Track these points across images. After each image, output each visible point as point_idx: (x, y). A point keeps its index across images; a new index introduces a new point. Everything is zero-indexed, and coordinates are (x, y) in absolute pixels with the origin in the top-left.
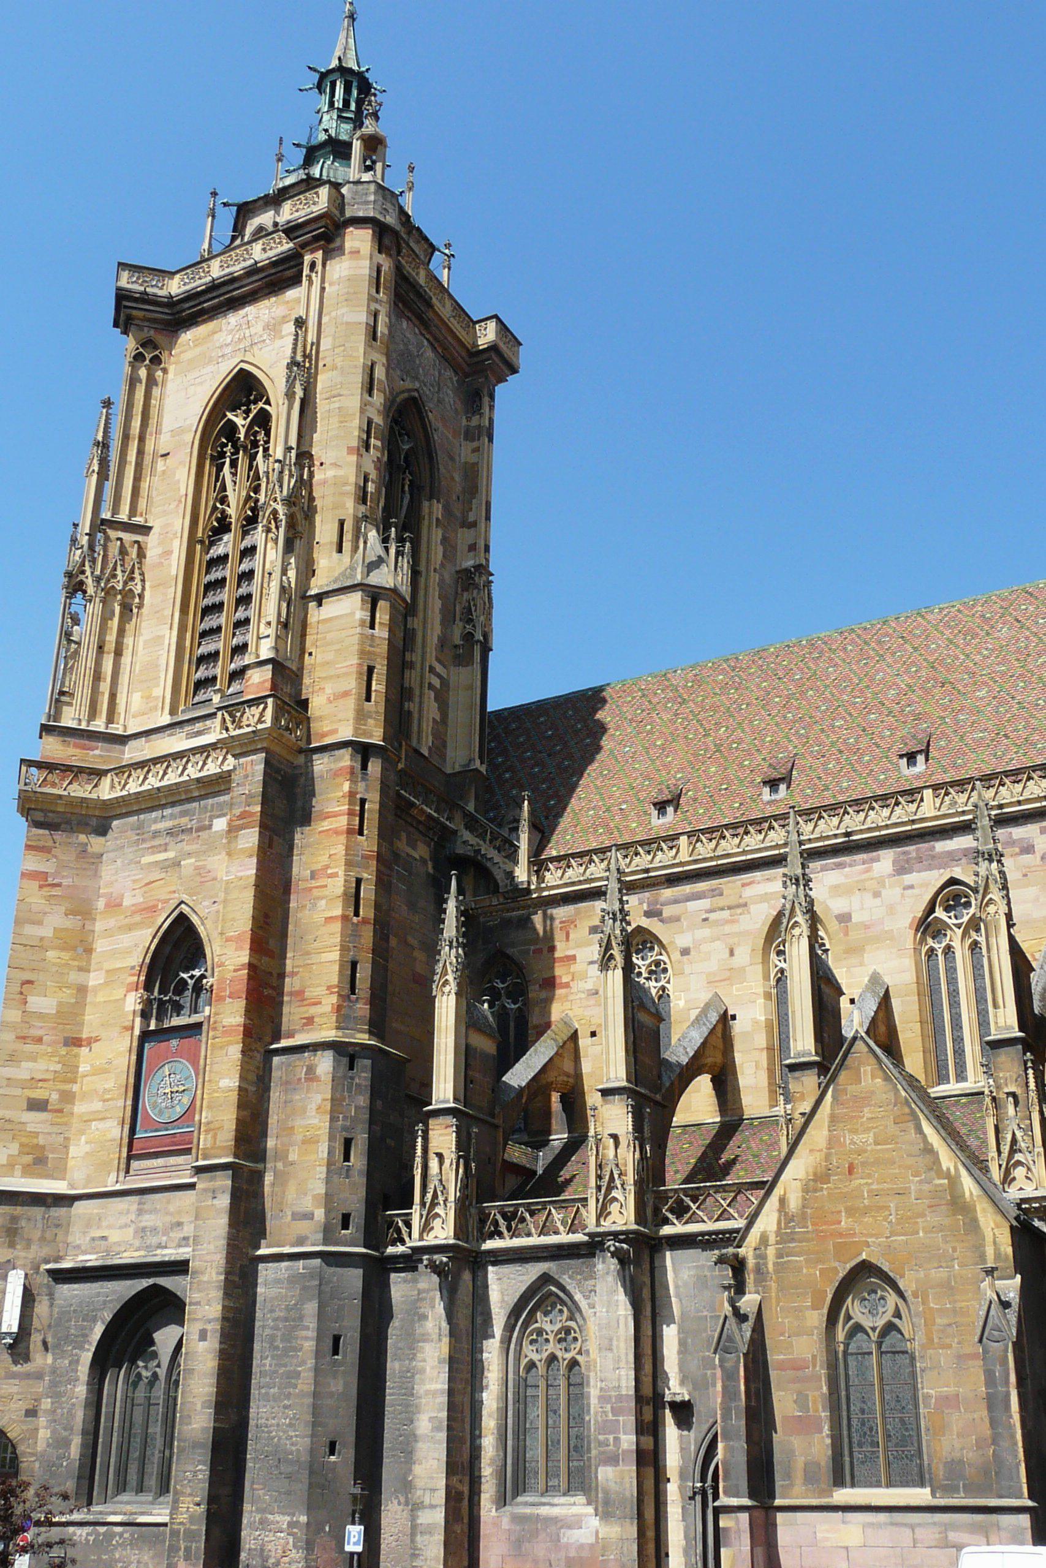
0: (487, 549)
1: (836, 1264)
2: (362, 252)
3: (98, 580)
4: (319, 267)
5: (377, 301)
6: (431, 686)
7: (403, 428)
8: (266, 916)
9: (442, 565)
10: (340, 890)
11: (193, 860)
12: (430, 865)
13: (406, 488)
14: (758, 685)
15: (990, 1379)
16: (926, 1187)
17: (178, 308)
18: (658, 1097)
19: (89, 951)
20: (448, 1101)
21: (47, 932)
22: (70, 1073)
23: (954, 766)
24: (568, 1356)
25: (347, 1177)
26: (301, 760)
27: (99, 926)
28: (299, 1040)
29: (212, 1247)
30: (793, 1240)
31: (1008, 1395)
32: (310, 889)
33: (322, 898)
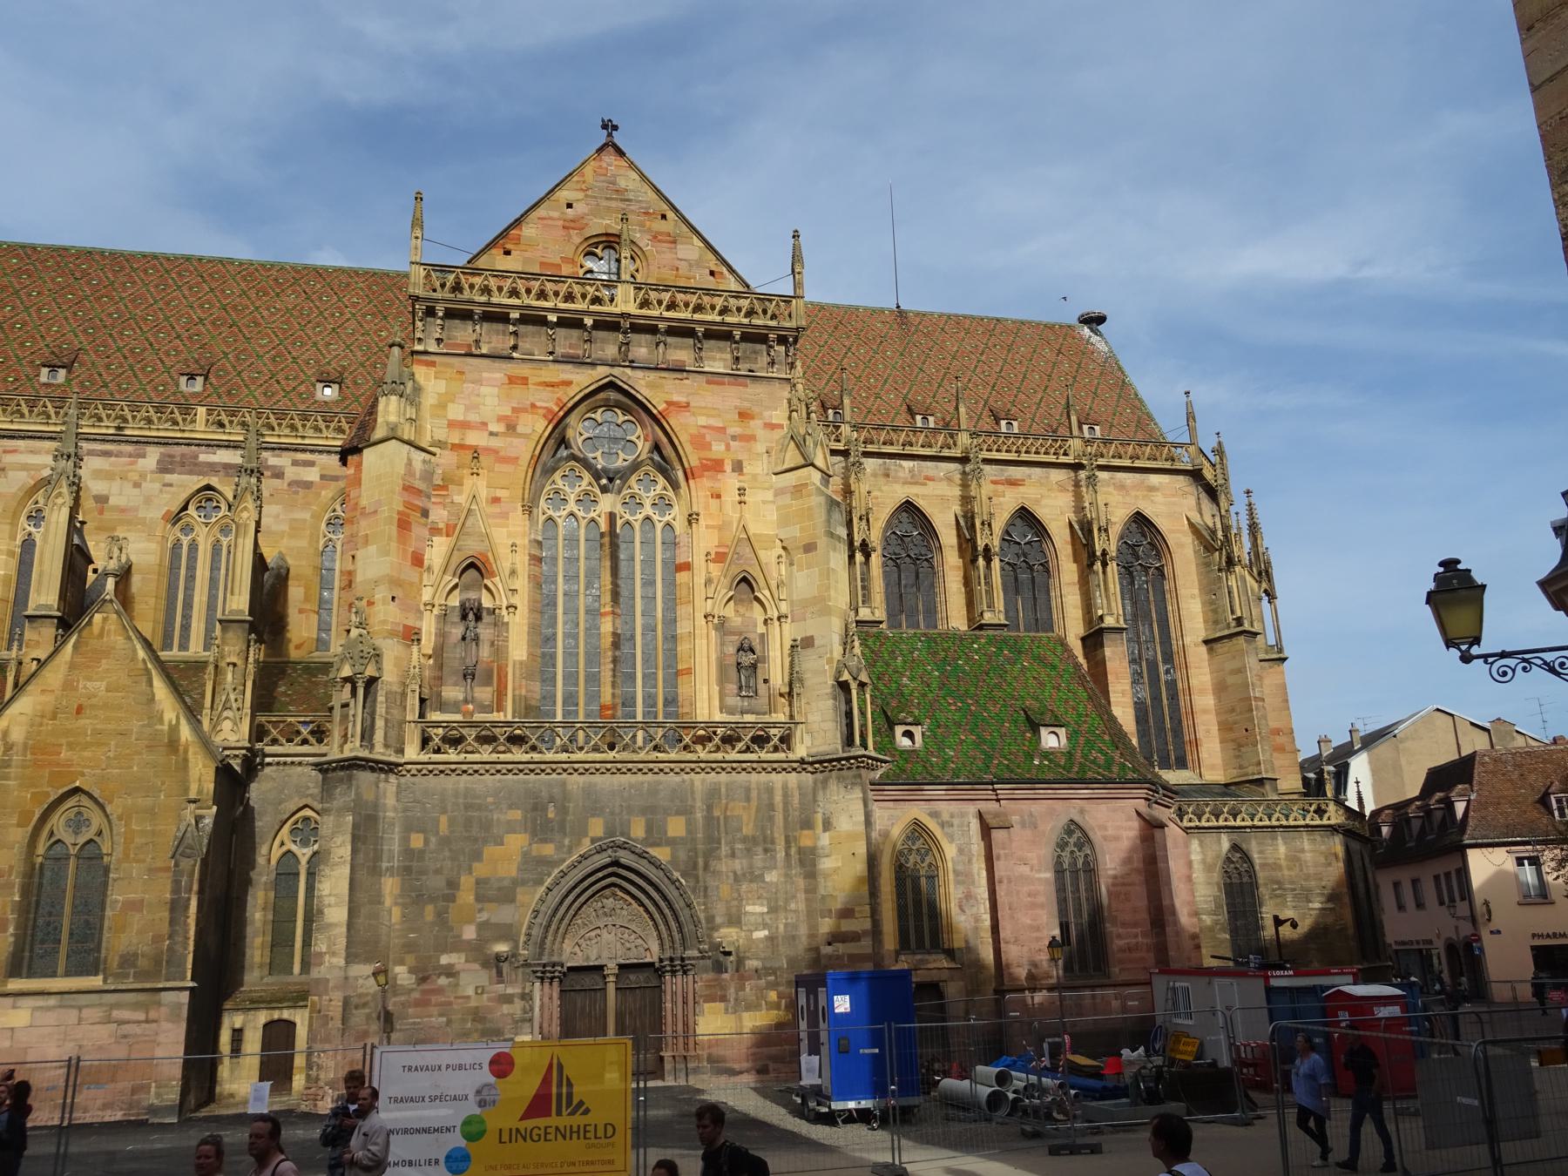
1: (49, 789)
14: (53, 280)
15: (176, 888)
30: (9, 766)
31: (189, 899)
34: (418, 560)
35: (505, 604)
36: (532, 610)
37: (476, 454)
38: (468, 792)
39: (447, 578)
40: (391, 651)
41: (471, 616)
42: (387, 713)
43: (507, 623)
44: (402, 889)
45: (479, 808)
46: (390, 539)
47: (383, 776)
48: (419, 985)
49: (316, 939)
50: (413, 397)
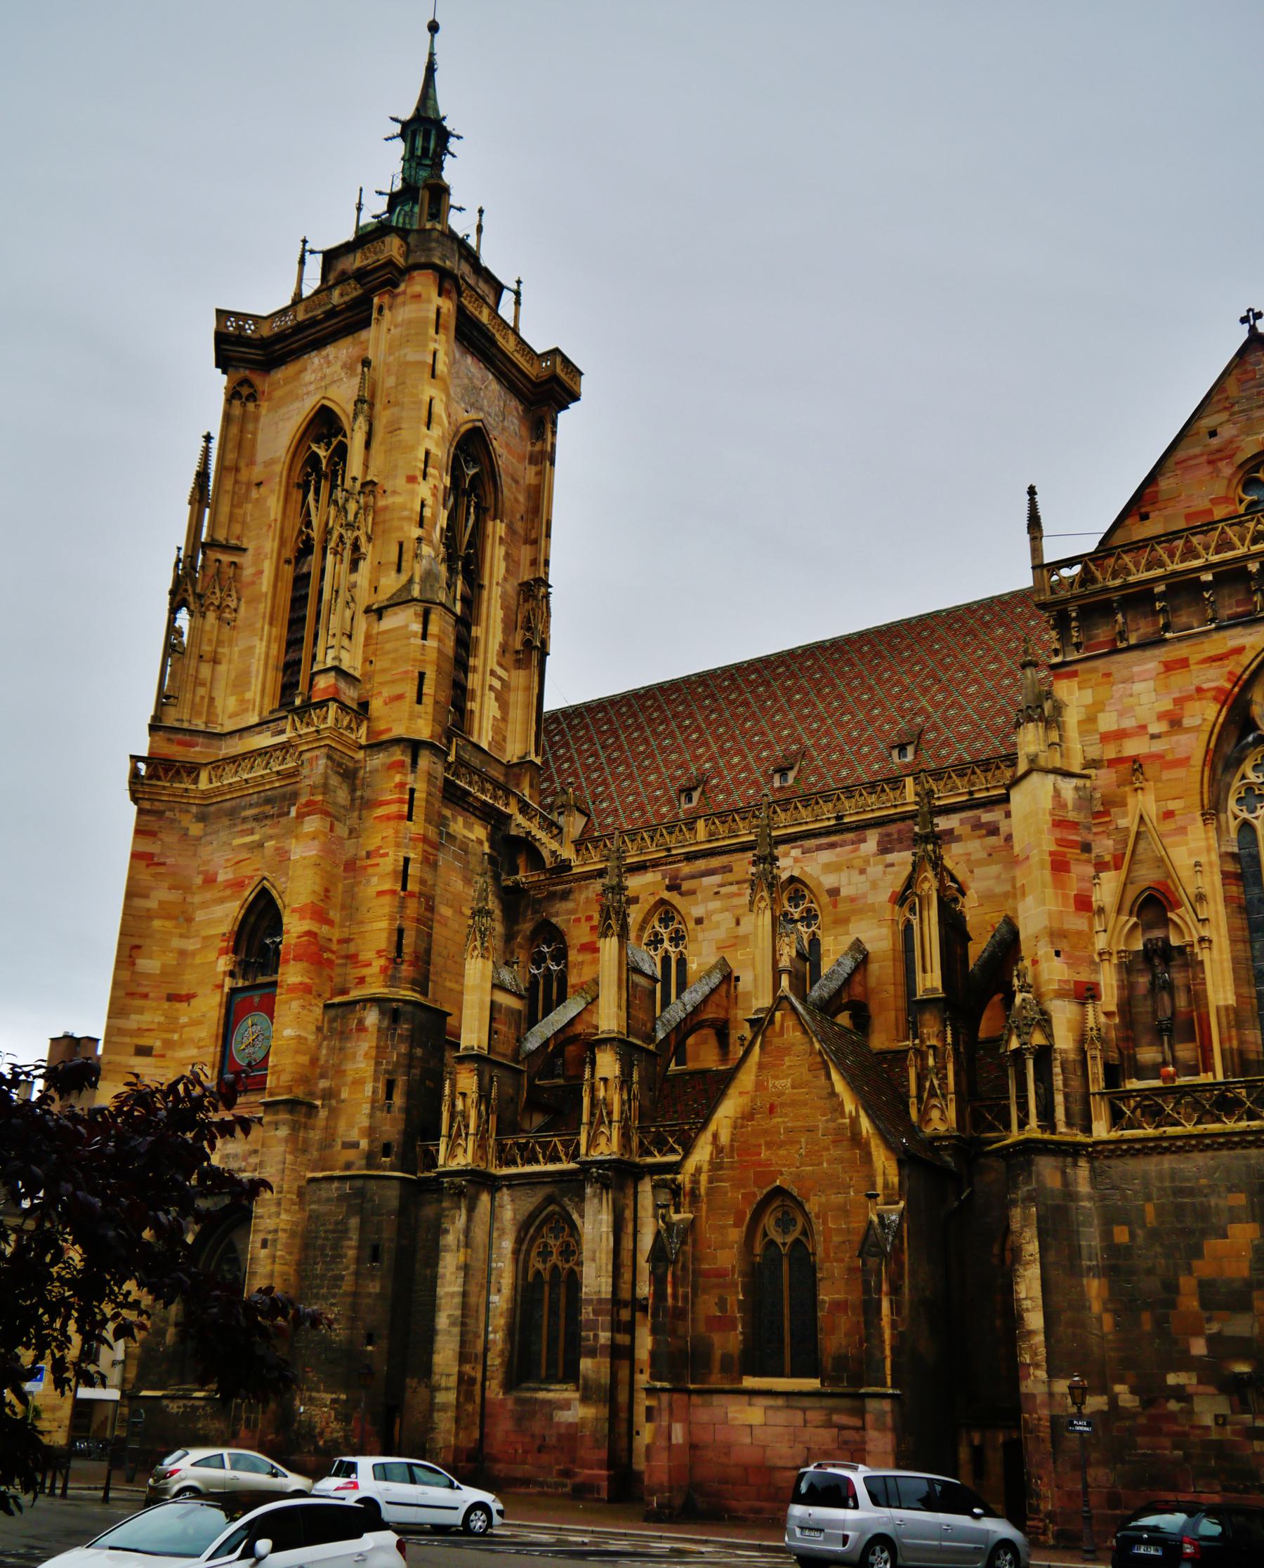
0: (547, 563)
3: (199, 596)
6: (491, 688)
7: (468, 455)
8: (327, 890)
9: (505, 579)
10: (390, 868)
11: (273, 843)
12: (486, 845)
13: (472, 510)
16: (832, 1125)
18: (652, 1047)
19: (189, 920)
20: (472, 1048)
21: (152, 904)
22: (171, 1025)
23: (936, 757)
24: (567, 1266)
25: (389, 1112)
26: (360, 755)
27: (197, 899)
28: (355, 994)
29: (273, 1171)
30: (721, 1168)
31: (880, 1301)
32: (365, 868)
33: (374, 875)
34: (1083, 903)
35: (1195, 940)
36: (1233, 941)
37: (1136, 765)
38: (1173, 1175)
39: (1124, 918)
40: (1063, 1015)
41: (1157, 962)
42: (1065, 1085)
43: (1202, 962)
44: (1111, 1289)
45: (1191, 1192)
46: (1044, 886)
47: (1069, 1160)
48: (1144, 1409)
49: (1021, 1349)
50: (1053, 721)
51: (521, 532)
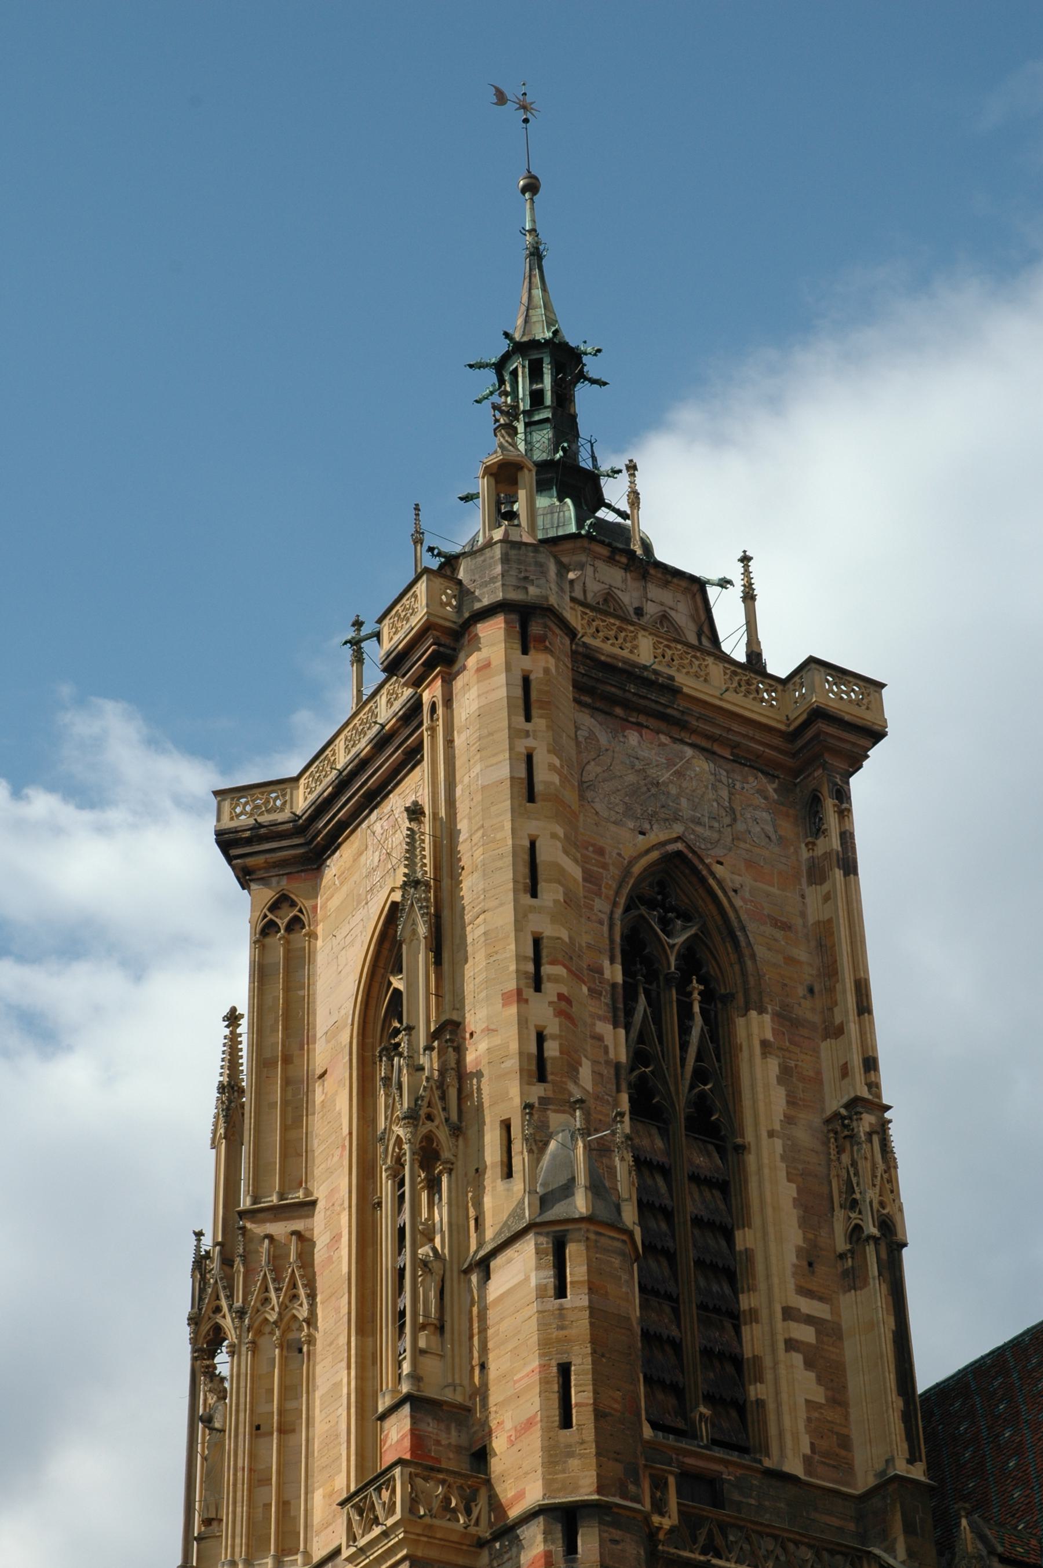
0: (871, 1064)
2: (494, 664)
3: (241, 1313)
4: (440, 711)
5: (527, 734)
6: (791, 1345)
9: (789, 1120)
17: (312, 831)
51: (816, 1019)
